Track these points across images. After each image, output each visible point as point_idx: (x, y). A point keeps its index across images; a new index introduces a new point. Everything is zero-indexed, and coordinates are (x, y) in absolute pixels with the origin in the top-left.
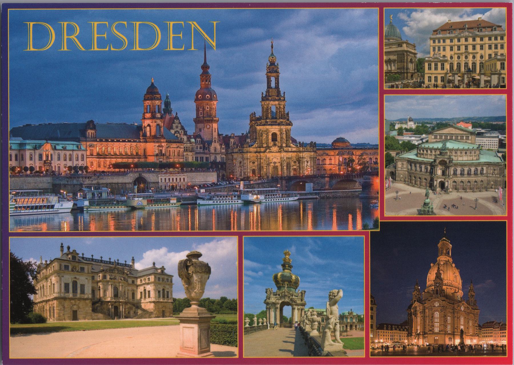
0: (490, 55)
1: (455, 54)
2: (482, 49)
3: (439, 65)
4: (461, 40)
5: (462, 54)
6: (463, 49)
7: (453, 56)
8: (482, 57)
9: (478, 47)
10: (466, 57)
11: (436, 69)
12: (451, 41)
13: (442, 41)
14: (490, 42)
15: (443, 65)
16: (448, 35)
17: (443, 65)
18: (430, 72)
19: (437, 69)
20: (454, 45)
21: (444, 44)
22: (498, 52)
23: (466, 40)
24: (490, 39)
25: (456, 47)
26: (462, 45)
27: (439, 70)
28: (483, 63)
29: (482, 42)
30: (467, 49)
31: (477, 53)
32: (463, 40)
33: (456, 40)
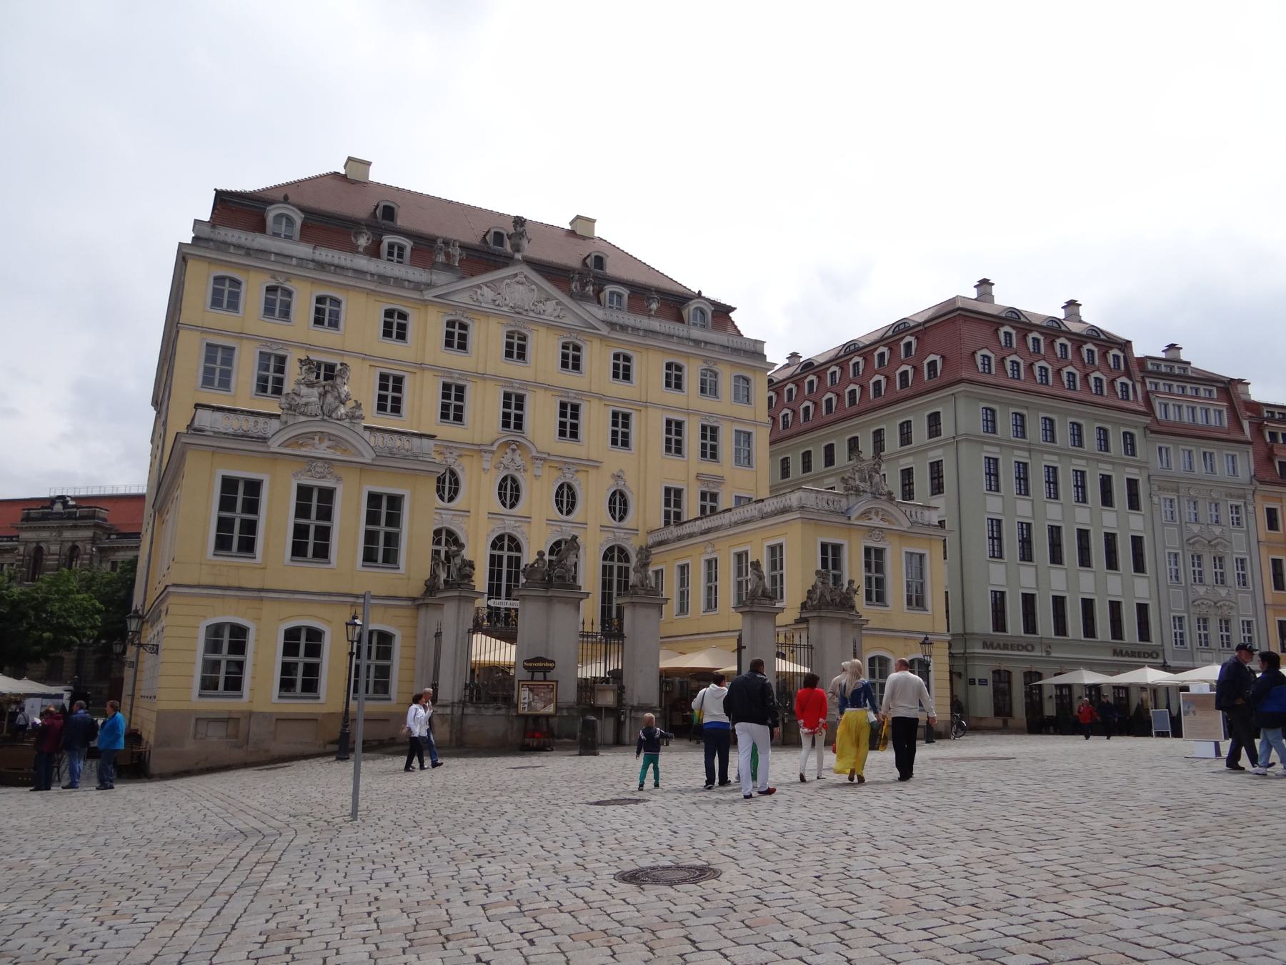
0: (673, 496)
2: (625, 444)
4: (475, 336)
6: (484, 409)
8: (619, 504)
9: (595, 422)
10: (510, 491)
11: (311, 542)
14: (673, 397)
17: (384, 510)
19: (322, 552)
21: (323, 336)
22: (720, 480)
23: (516, 349)
24: (674, 379)
28: (623, 554)
29: (619, 389)
30: (519, 426)
31: (594, 464)
32: (487, 338)
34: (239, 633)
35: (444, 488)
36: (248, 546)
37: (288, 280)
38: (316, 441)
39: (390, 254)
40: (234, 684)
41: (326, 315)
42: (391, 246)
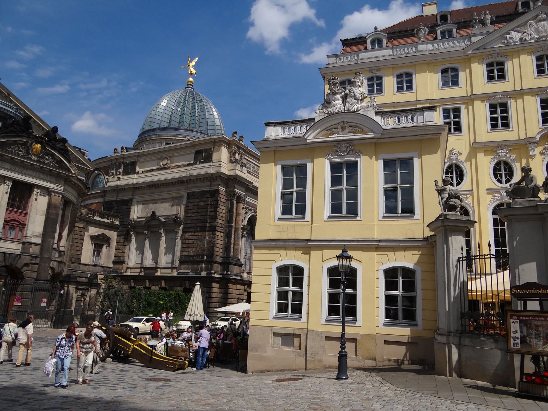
1: (477, 147)
3: (372, 175)
4: (509, 66)
5: (524, 146)
7: (466, 167)
11: (345, 205)
12: (450, 76)
13: (390, 83)
15: (399, 169)
16: (425, 48)
18: (297, 230)
19: (353, 210)
20: (470, 99)
25: (482, 111)
26: (520, 94)
27: (373, 217)
33: (479, 70)
34: (298, 271)
35: (501, 175)
36: (301, 211)
37: (379, 70)
38: (340, 130)
39: (443, 37)
40: (298, 309)
41: (405, 82)
42: (443, 33)
